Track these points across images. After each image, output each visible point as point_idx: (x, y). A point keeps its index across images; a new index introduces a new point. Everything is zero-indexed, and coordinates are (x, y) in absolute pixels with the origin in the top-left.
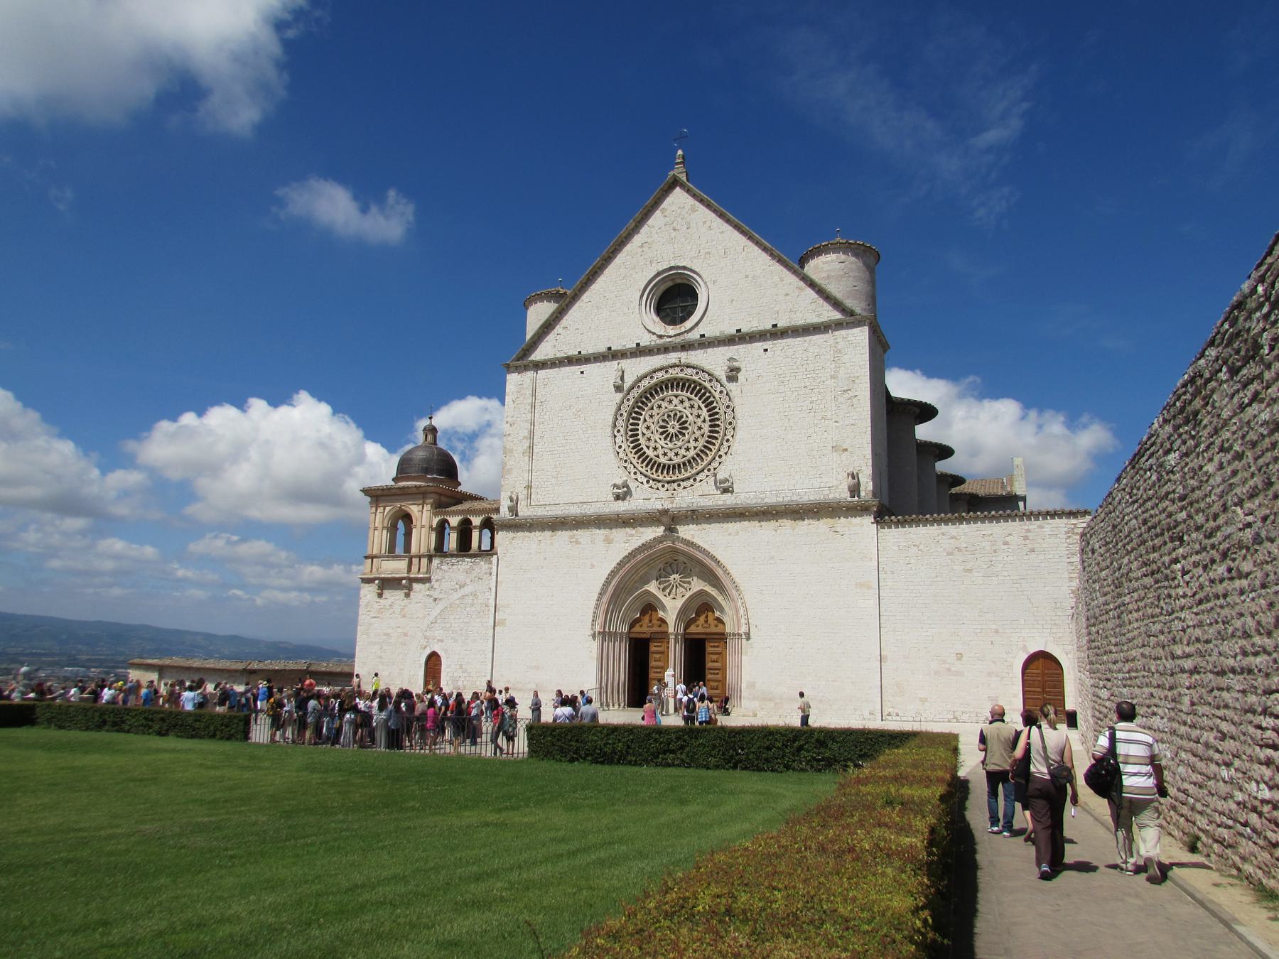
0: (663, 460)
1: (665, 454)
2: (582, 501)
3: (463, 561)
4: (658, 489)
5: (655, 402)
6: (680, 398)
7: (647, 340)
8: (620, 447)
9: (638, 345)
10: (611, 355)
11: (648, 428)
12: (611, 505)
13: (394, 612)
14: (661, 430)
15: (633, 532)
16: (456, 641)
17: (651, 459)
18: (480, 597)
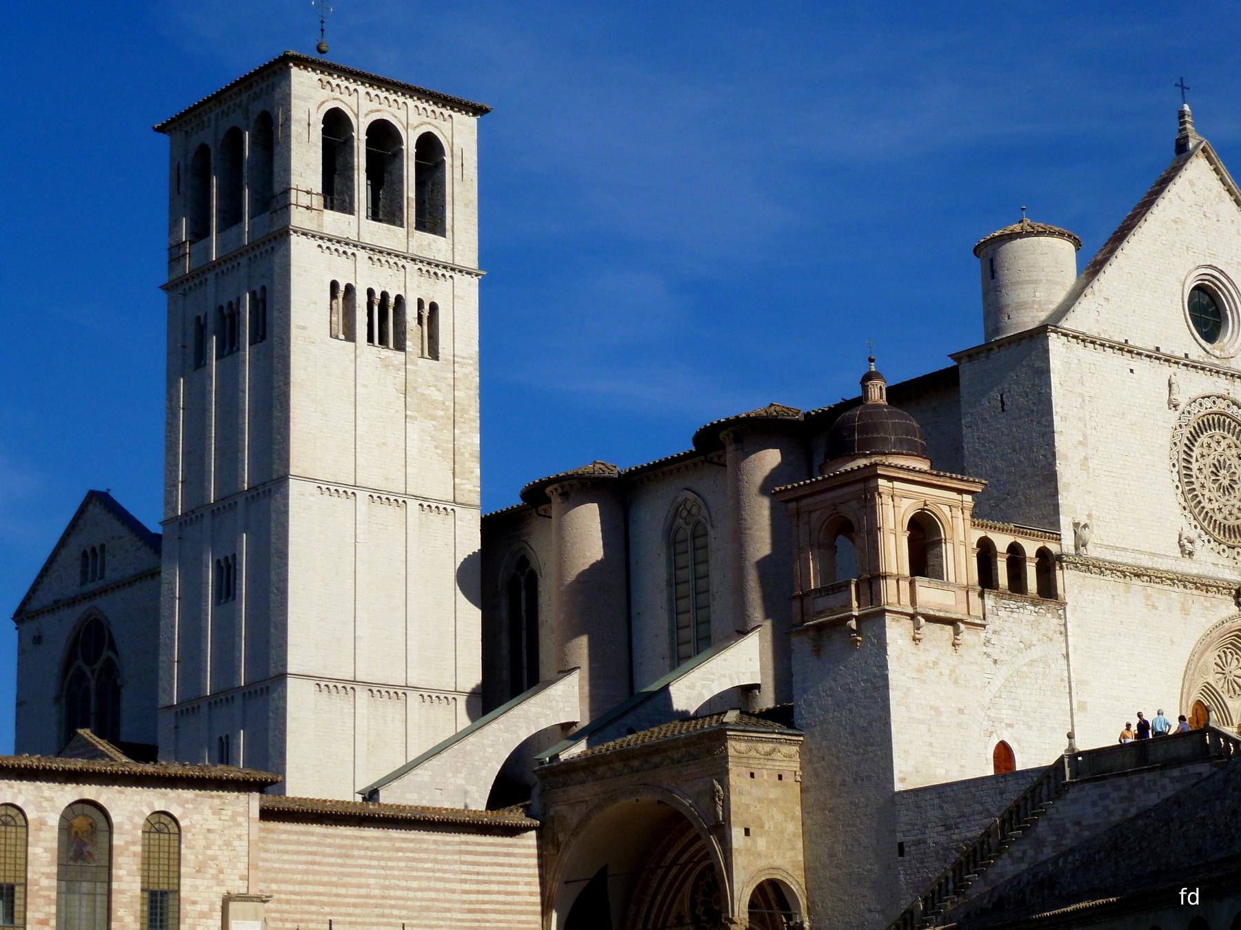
0: (1219, 517)
1: (1220, 509)
2: (1149, 550)
3: (1024, 607)
4: (1219, 553)
5: (1204, 438)
6: (1227, 441)
7: (1196, 353)
8: (1177, 487)
9: (1186, 355)
10: (1156, 355)
11: (1200, 469)
12: (1183, 564)
13: (941, 674)
14: (1214, 478)
15: (1208, 604)
16: (1030, 727)
17: (1207, 513)
18: (1053, 666)
